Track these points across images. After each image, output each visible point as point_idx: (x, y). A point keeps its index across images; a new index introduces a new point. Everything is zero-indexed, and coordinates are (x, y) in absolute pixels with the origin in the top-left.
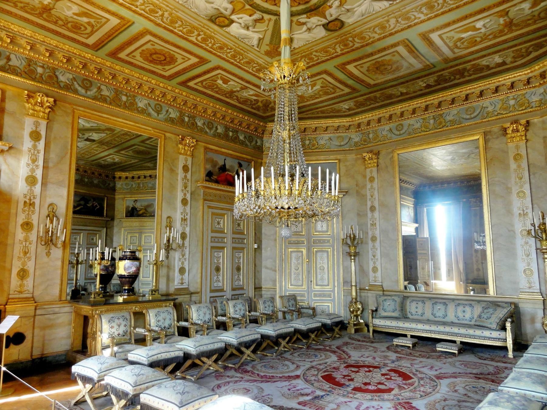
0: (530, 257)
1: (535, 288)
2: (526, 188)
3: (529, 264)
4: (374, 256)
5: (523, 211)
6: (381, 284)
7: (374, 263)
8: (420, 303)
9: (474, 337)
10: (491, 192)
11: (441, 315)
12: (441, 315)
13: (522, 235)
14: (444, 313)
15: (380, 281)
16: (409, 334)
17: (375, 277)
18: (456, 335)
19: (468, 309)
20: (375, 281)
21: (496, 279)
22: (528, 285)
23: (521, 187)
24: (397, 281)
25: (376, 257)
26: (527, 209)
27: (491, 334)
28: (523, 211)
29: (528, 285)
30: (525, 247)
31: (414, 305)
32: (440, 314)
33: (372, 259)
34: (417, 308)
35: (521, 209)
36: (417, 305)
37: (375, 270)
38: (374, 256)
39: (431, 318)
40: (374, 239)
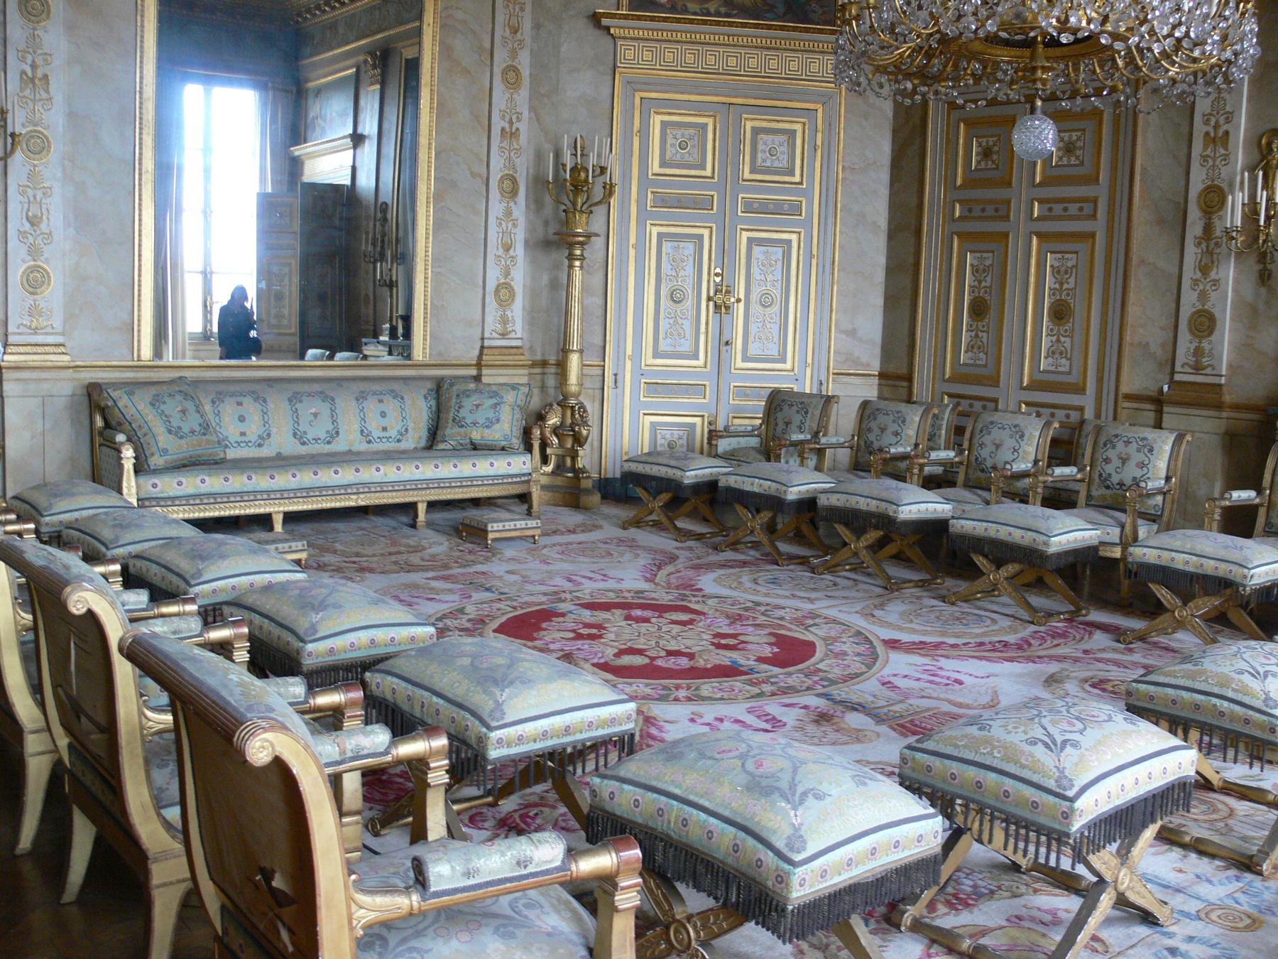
0: (511, 252)
1: (512, 335)
2: (524, 61)
3: (507, 274)
4: (34, 221)
5: (511, 123)
6: (60, 339)
7: (34, 252)
8: (247, 401)
9: (322, 490)
10: (446, 51)
11: (323, 435)
12: (323, 435)
13: (502, 191)
14: (330, 427)
15: (57, 323)
16: (277, 509)
17: (33, 311)
18: (269, 495)
19: (391, 406)
20: (35, 331)
21: (436, 311)
22: (499, 327)
23: (514, 54)
24: (130, 328)
25: (43, 226)
26: (519, 120)
27: (509, 464)
28: (511, 123)
29: (499, 327)
30: (504, 225)
31: (229, 410)
32: (320, 430)
33: (21, 235)
34: (242, 419)
35: (507, 118)
36: (241, 411)
37: (36, 280)
38: (34, 221)
39: (290, 446)
40: (40, 146)
